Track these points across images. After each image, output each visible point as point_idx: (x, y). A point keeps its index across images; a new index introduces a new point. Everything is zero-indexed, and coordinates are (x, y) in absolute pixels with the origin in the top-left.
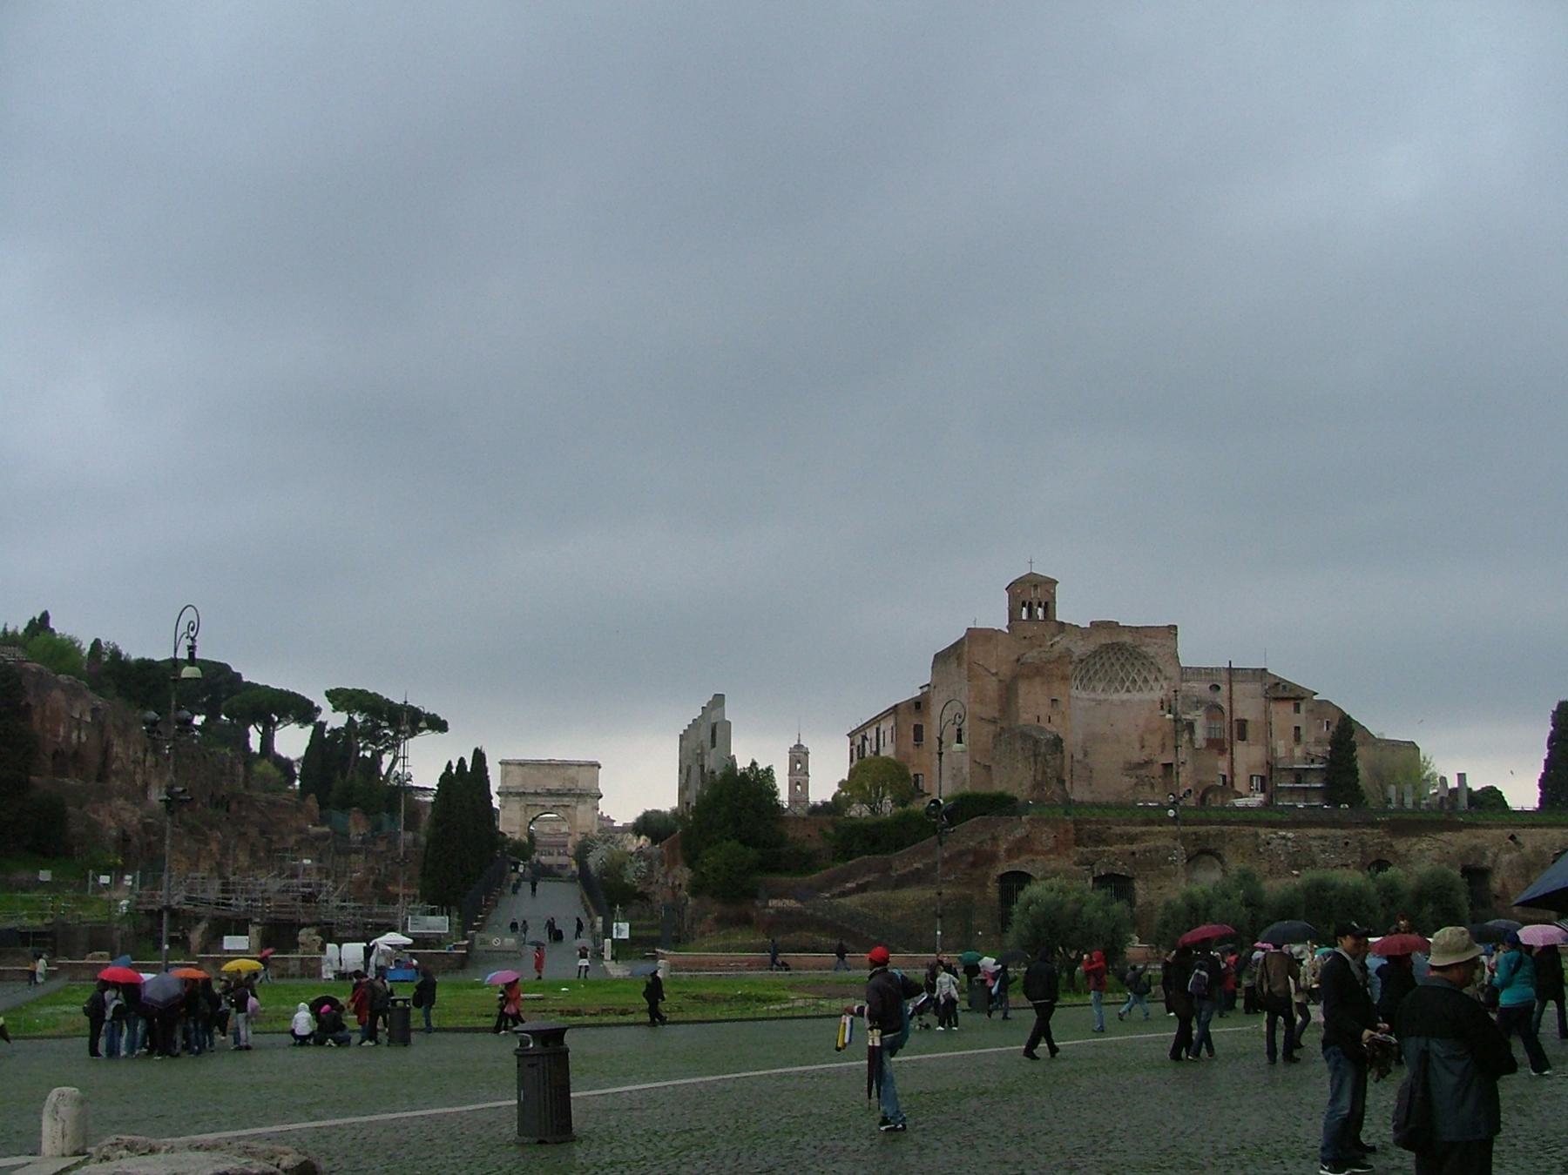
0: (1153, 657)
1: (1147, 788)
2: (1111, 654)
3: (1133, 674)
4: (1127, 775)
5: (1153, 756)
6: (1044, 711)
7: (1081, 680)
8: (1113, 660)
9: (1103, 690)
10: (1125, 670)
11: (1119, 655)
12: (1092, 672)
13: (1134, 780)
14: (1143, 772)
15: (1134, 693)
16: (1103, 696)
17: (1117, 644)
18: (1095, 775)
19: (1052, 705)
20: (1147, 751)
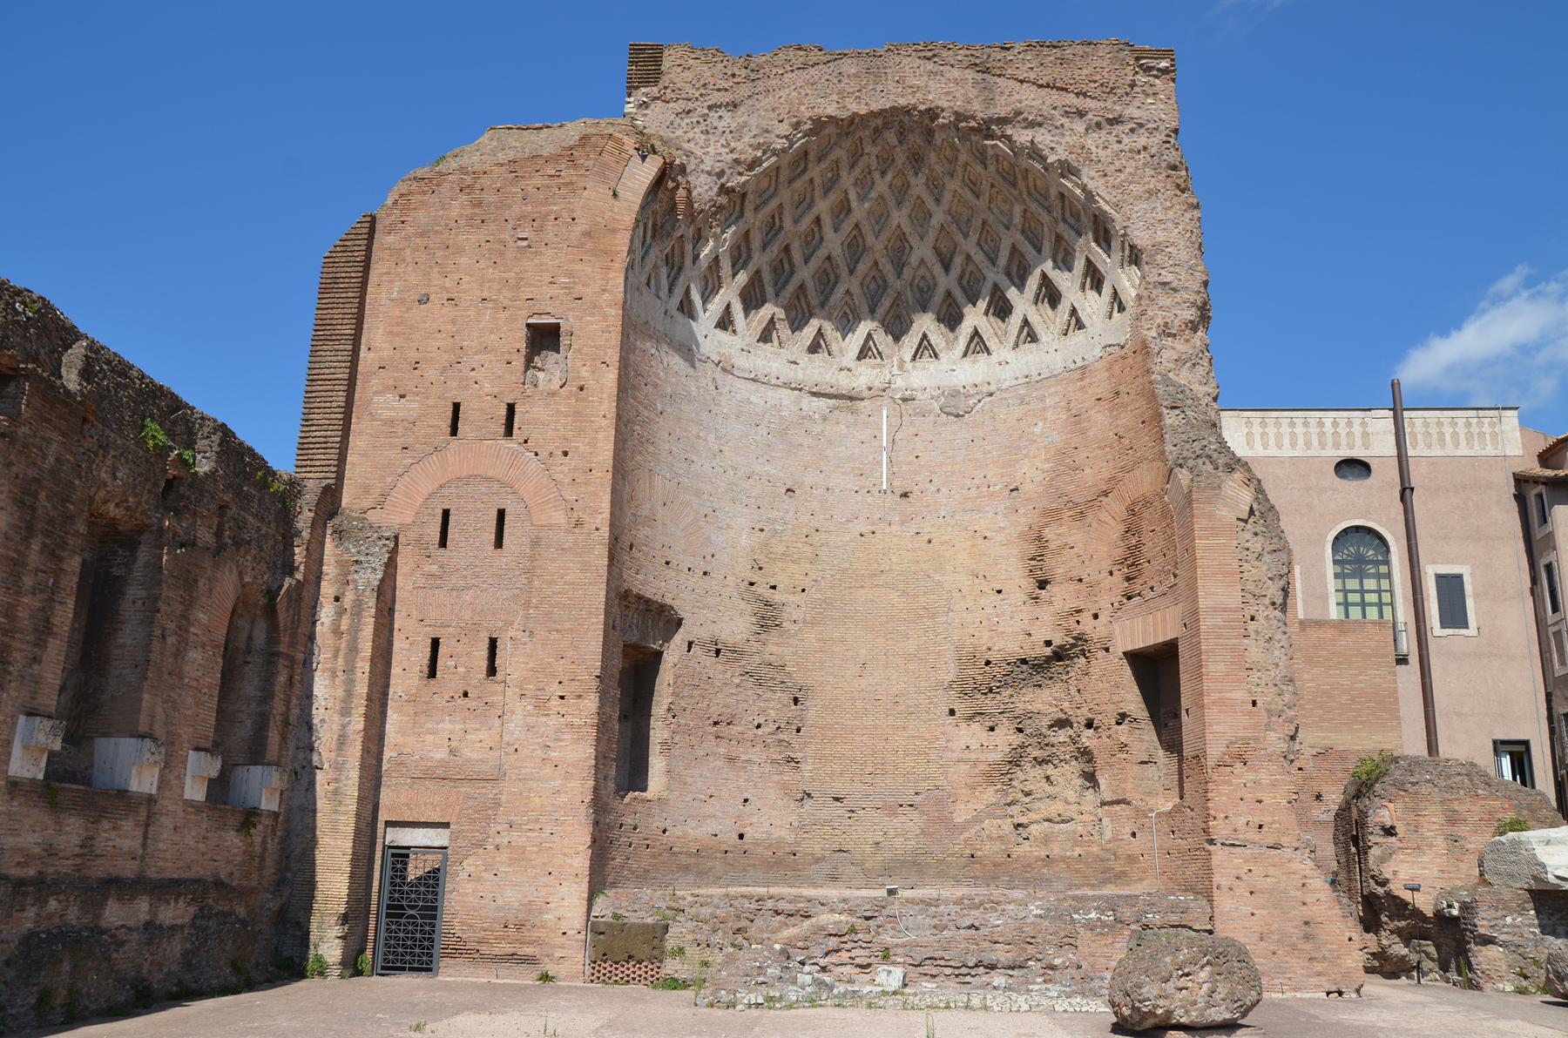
0: (1068, 169)
1: (1068, 775)
2: (881, 186)
4: (970, 718)
5: (1086, 618)
7: (752, 299)
10: (958, 260)
11: (918, 185)
12: (805, 274)
13: (1006, 738)
14: (1043, 700)
15: (1001, 352)
16: (865, 376)
17: (893, 119)
18: (812, 712)
20: (1061, 596)
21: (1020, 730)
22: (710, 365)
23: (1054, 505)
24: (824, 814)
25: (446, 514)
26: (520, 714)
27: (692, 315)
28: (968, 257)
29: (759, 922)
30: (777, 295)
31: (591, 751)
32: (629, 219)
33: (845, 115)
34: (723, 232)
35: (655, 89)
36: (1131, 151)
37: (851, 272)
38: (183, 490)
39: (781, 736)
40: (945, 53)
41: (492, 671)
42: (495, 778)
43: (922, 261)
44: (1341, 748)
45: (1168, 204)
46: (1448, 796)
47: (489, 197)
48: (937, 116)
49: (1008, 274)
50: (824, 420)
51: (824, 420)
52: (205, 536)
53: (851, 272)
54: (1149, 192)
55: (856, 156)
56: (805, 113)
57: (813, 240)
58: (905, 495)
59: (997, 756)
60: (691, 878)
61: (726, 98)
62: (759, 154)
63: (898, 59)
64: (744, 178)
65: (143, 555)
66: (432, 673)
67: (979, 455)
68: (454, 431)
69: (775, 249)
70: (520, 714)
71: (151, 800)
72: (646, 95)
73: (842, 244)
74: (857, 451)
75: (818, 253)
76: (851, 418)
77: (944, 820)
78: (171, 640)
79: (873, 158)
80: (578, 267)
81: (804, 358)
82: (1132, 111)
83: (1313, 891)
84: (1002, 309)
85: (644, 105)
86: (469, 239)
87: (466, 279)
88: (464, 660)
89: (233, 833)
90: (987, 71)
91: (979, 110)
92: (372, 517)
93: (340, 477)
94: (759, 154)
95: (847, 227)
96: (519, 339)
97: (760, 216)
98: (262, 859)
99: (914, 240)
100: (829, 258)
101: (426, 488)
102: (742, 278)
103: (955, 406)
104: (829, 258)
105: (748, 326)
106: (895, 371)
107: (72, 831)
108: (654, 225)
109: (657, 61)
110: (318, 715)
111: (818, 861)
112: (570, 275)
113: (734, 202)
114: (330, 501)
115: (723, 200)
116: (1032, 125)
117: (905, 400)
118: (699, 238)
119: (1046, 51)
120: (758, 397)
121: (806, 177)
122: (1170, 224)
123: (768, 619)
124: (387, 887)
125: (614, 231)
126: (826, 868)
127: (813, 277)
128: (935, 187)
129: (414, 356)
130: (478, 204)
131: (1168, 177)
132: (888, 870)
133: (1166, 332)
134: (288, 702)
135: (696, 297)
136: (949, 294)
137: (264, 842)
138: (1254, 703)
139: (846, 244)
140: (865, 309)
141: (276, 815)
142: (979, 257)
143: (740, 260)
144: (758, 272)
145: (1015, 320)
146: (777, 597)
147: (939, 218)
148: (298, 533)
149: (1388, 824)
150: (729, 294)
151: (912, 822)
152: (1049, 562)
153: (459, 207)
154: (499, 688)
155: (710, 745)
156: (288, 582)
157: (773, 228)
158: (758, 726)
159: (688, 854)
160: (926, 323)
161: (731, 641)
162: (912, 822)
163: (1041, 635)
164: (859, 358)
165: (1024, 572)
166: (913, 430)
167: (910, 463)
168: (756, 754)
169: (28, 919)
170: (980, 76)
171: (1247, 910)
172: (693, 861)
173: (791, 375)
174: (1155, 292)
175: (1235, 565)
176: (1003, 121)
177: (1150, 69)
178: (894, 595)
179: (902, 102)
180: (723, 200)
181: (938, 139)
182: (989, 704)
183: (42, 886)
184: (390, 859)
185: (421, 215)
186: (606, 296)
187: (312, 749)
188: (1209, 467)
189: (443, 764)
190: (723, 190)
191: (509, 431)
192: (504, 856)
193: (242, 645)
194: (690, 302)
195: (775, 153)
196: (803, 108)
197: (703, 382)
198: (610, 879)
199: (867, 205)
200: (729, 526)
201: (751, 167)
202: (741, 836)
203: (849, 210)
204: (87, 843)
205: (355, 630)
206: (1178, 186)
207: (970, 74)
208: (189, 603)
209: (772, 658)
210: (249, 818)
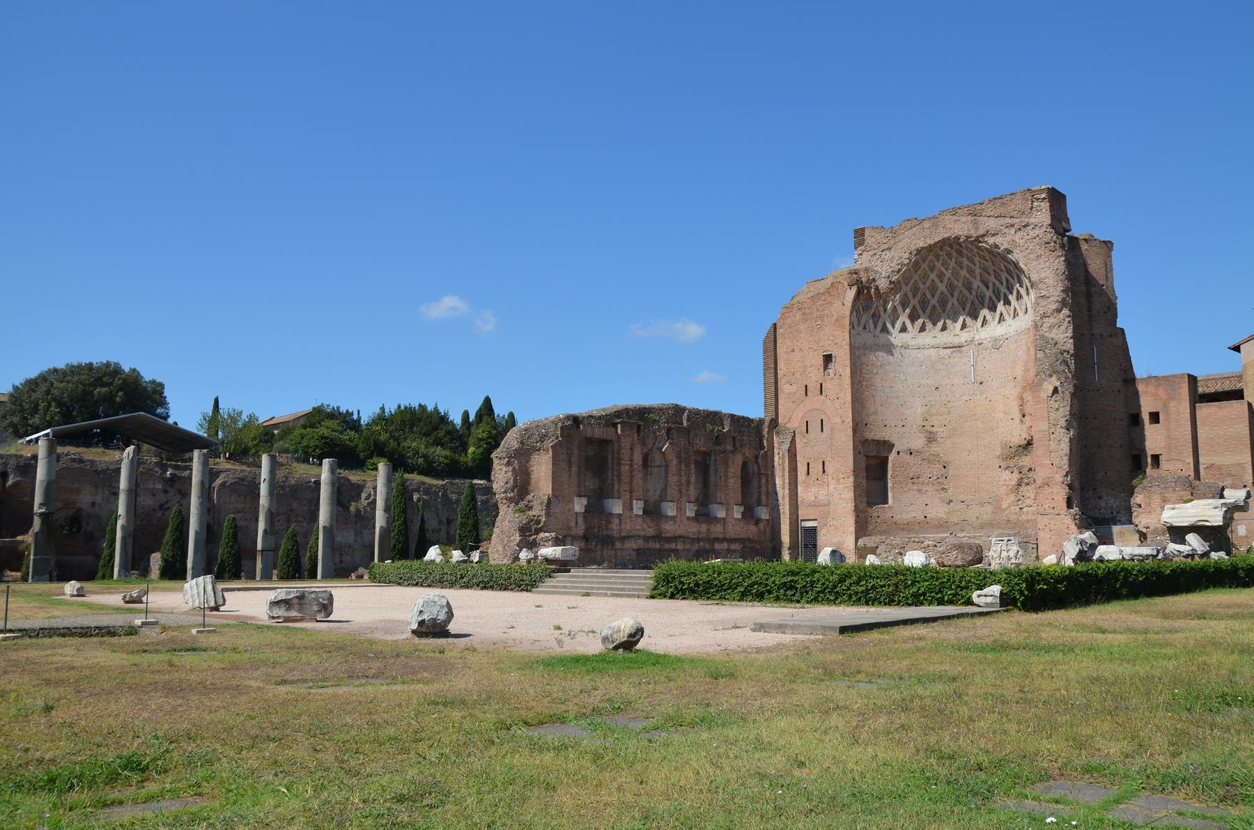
0: (1009, 252)
3: (1003, 290)
6: (814, 375)
7: (913, 318)
8: (964, 273)
9: (964, 326)
10: (991, 285)
11: (965, 261)
12: (934, 301)
13: (1016, 476)
14: (1026, 461)
16: (964, 336)
17: (944, 242)
18: (951, 471)
19: (826, 367)
21: (1021, 472)
22: (898, 348)
23: (1025, 385)
24: (957, 507)
25: (807, 422)
26: (833, 484)
27: (888, 332)
28: (994, 283)
29: (909, 545)
30: (924, 312)
31: (853, 494)
32: (848, 313)
33: (927, 245)
34: (895, 297)
35: (863, 247)
36: (1032, 238)
37: (952, 296)
38: (721, 438)
39: (939, 481)
40: (959, 211)
41: (824, 472)
42: (828, 504)
43: (978, 287)
44: (1218, 464)
45: (1047, 259)
46: (1163, 491)
47: (807, 311)
48: (959, 239)
49: (1008, 288)
50: (950, 357)
51: (950, 357)
52: (729, 448)
53: (952, 296)
54: (1038, 257)
55: (937, 257)
56: (913, 248)
57: (933, 289)
58: (981, 383)
59: (1014, 483)
60: (905, 532)
61: (886, 246)
62: (900, 267)
63: (943, 217)
64: (897, 277)
65: (712, 457)
66: (808, 474)
67: (1005, 365)
68: (806, 395)
69: (919, 296)
70: (833, 484)
71: (724, 519)
72: (861, 250)
73: (946, 286)
74: (963, 368)
75: (937, 292)
76: (960, 355)
77: (999, 507)
78: (723, 478)
79: (945, 256)
80: (835, 332)
81: (939, 335)
82: (1032, 220)
83: (1070, 530)
84: (1007, 302)
85: (861, 254)
86: (802, 327)
87: (804, 342)
88: (816, 468)
89: (752, 526)
90: (975, 215)
91: (974, 234)
92: (788, 425)
93: (777, 414)
94: (900, 267)
95: (945, 281)
96: (821, 361)
97: (908, 287)
98: (765, 533)
99: (972, 280)
100: (942, 293)
101: (801, 414)
102: (908, 311)
103: (997, 344)
104: (942, 293)
105: (912, 329)
106: (975, 332)
107: (704, 527)
108: (863, 307)
109: (863, 235)
110: (778, 489)
111: (956, 524)
112: (833, 336)
113: (895, 286)
114: (774, 423)
115: (892, 286)
116: (993, 235)
117: (979, 344)
118: (886, 302)
119: (997, 201)
120: (920, 355)
121: (922, 269)
122: (1046, 269)
123: (931, 438)
124: (803, 539)
125: (844, 318)
126: (959, 527)
127: (938, 302)
128: (971, 260)
129: (793, 370)
130: (804, 314)
131: (1046, 247)
132: (982, 527)
133: (1044, 316)
134: (767, 487)
135: (889, 326)
136: (991, 298)
137: (764, 527)
138: (1052, 464)
139: (948, 286)
140: (961, 309)
141: (768, 520)
142: (997, 283)
143: (904, 305)
144: (914, 306)
145: (1012, 308)
146: (934, 429)
147: (978, 271)
148: (764, 436)
149: (1139, 503)
150: (904, 318)
151: (988, 509)
152: (1025, 407)
153: (799, 316)
154: (826, 476)
155: (910, 486)
156: (762, 452)
157: (915, 290)
158: (930, 478)
159: (905, 524)
160: (985, 312)
161: (916, 448)
162: (988, 509)
163: (1023, 437)
164: (962, 329)
165: (1018, 412)
166: (982, 356)
167: (982, 370)
168: (930, 488)
169: (696, 547)
170: (973, 218)
171: (1048, 536)
172: (906, 526)
173: (934, 342)
174: (1039, 301)
175: (1046, 414)
176: (983, 236)
177: (1039, 199)
178: (979, 423)
179: (946, 236)
180: (892, 286)
181: (964, 245)
182: (1011, 463)
183: (699, 540)
184: (803, 531)
185: (788, 321)
186: (844, 342)
187: (777, 500)
188: (1044, 376)
189: (814, 501)
190: (891, 282)
191: (821, 393)
192: (832, 528)
193: (751, 472)
194: (887, 327)
195: (905, 265)
196: (912, 246)
197: (896, 355)
198: (868, 534)
199: (950, 271)
200: (912, 406)
201: (898, 273)
202: (926, 517)
203: (944, 275)
204: (708, 530)
205: (783, 463)
206: (1051, 250)
207: (970, 218)
208: (727, 466)
209: (934, 453)
210: (758, 522)
